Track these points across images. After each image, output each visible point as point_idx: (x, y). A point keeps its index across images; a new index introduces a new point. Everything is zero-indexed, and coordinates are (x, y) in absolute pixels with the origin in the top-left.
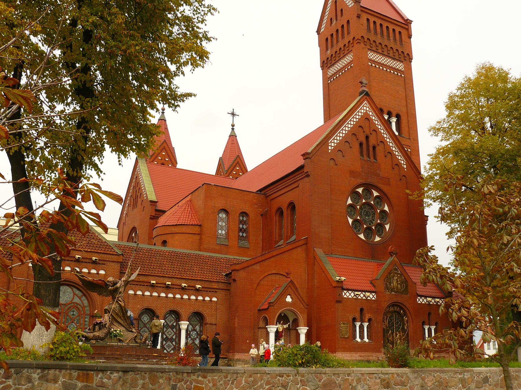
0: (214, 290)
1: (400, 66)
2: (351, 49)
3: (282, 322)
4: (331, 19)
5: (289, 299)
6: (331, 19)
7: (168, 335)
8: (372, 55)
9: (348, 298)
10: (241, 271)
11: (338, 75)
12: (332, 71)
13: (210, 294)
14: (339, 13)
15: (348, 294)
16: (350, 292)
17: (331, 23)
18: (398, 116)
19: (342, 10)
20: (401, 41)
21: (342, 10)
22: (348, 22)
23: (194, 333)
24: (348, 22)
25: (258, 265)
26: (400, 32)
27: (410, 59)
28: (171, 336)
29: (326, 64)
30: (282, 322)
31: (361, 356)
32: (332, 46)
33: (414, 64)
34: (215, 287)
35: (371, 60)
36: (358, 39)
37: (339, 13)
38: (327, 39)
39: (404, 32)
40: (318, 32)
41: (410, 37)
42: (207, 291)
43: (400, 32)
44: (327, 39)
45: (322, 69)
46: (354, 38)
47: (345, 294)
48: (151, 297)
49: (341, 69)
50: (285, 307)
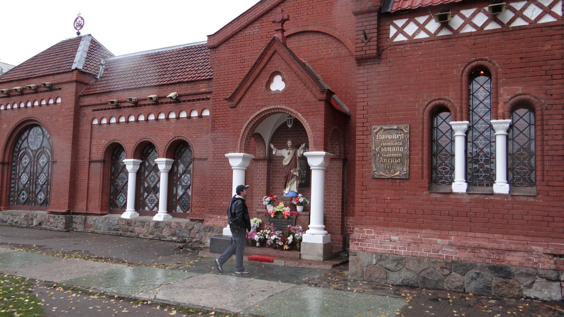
0: (204, 96)
3: (289, 143)
5: (278, 85)
7: (151, 183)
9: (412, 42)
10: (222, 48)
13: (197, 104)
15: (411, 29)
16: (421, 20)
23: (186, 178)
25: (257, 24)
28: (154, 183)
30: (289, 143)
31: (461, 248)
34: (203, 90)
42: (194, 100)
47: (400, 31)
48: (118, 125)
50: (263, 106)
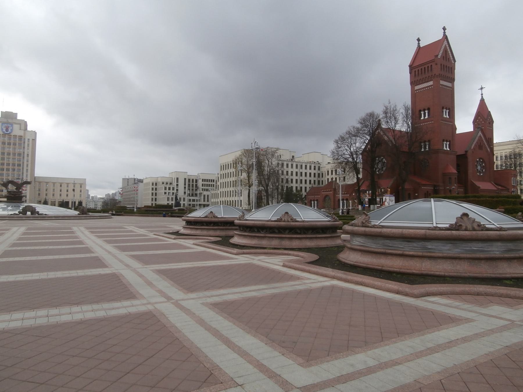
2: (432, 79)
8: (442, 82)
11: (423, 90)
20: (451, 72)
33: (455, 83)
35: (442, 85)
36: (438, 75)
46: (435, 74)
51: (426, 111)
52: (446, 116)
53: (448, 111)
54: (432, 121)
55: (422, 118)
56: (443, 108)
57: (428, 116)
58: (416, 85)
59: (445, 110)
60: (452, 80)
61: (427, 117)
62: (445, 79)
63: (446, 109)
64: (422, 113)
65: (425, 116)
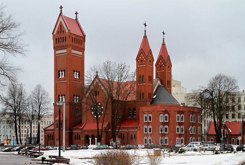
1: (80, 53)
4: (59, 32)
6: (59, 32)
8: (73, 51)
12: (58, 52)
14: (62, 32)
17: (59, 33)
18: (79, 72)
19: (63, 31)
20: (82, 44)
21: (63, 31)
22: (66, 37)
24: (66, 37)
26: (82, 40)
27: (84, 50)
29: (56, 48)
32: (59, 42)
37: (62, 32)
38: (56, 39)
39: (83, 40)
40: (53, 33)
41: (85, 41)
43: (82, 40)
44: (56, 39)
45: (54, 49)
49: (62, 53)
51: (63, 72)
52: (76, 76)
53: (78, 73)
54: (66, 80)
55: (60, 77)
56: (74, 71)
57: (65, 76)
58: (57, 50)
59: (75, 73)
60: (83, 50)
61: (63, 77)
62: (77, 50)
63: (77, 72)
64: (60, 72)
65: (62, 76)
